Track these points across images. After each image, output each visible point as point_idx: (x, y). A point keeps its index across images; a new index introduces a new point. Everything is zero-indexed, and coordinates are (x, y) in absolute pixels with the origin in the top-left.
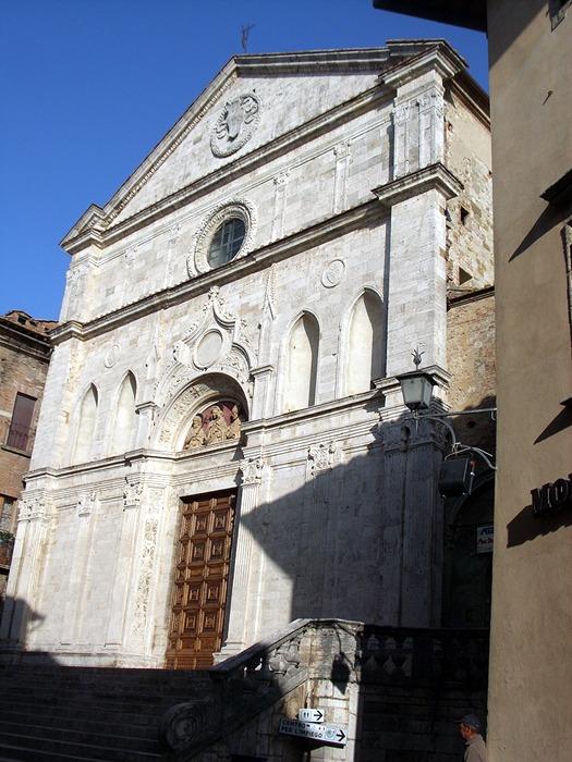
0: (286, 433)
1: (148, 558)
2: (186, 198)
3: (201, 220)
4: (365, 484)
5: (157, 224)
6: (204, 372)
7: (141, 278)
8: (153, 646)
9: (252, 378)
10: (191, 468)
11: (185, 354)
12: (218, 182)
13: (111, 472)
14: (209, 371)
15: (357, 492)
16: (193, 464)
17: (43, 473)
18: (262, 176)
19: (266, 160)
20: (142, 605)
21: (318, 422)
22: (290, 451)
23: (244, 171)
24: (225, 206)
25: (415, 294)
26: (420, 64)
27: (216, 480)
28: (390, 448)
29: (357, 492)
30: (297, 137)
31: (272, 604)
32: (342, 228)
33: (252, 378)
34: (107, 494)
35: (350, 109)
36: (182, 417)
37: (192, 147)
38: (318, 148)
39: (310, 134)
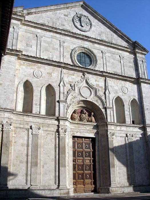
2: (68, 35)
4: (140, 146)
5: (55, 35)
6: (85, 99)
7: (46, 50)
10: (76, 127)
13: (48, 121)
14: (87, 99)
15: (138, 148)
16: (77, 126)
18: (96, 47)
19: (98, 44)
21: (127, 128)
23: (91, 41)
24: (85, 48)
26: (143, 53)
27: (87, 134)
29: (138, 148)
30: (110, 45)
31: (121, 173)
32: (127, 80)
37: (63, 16)
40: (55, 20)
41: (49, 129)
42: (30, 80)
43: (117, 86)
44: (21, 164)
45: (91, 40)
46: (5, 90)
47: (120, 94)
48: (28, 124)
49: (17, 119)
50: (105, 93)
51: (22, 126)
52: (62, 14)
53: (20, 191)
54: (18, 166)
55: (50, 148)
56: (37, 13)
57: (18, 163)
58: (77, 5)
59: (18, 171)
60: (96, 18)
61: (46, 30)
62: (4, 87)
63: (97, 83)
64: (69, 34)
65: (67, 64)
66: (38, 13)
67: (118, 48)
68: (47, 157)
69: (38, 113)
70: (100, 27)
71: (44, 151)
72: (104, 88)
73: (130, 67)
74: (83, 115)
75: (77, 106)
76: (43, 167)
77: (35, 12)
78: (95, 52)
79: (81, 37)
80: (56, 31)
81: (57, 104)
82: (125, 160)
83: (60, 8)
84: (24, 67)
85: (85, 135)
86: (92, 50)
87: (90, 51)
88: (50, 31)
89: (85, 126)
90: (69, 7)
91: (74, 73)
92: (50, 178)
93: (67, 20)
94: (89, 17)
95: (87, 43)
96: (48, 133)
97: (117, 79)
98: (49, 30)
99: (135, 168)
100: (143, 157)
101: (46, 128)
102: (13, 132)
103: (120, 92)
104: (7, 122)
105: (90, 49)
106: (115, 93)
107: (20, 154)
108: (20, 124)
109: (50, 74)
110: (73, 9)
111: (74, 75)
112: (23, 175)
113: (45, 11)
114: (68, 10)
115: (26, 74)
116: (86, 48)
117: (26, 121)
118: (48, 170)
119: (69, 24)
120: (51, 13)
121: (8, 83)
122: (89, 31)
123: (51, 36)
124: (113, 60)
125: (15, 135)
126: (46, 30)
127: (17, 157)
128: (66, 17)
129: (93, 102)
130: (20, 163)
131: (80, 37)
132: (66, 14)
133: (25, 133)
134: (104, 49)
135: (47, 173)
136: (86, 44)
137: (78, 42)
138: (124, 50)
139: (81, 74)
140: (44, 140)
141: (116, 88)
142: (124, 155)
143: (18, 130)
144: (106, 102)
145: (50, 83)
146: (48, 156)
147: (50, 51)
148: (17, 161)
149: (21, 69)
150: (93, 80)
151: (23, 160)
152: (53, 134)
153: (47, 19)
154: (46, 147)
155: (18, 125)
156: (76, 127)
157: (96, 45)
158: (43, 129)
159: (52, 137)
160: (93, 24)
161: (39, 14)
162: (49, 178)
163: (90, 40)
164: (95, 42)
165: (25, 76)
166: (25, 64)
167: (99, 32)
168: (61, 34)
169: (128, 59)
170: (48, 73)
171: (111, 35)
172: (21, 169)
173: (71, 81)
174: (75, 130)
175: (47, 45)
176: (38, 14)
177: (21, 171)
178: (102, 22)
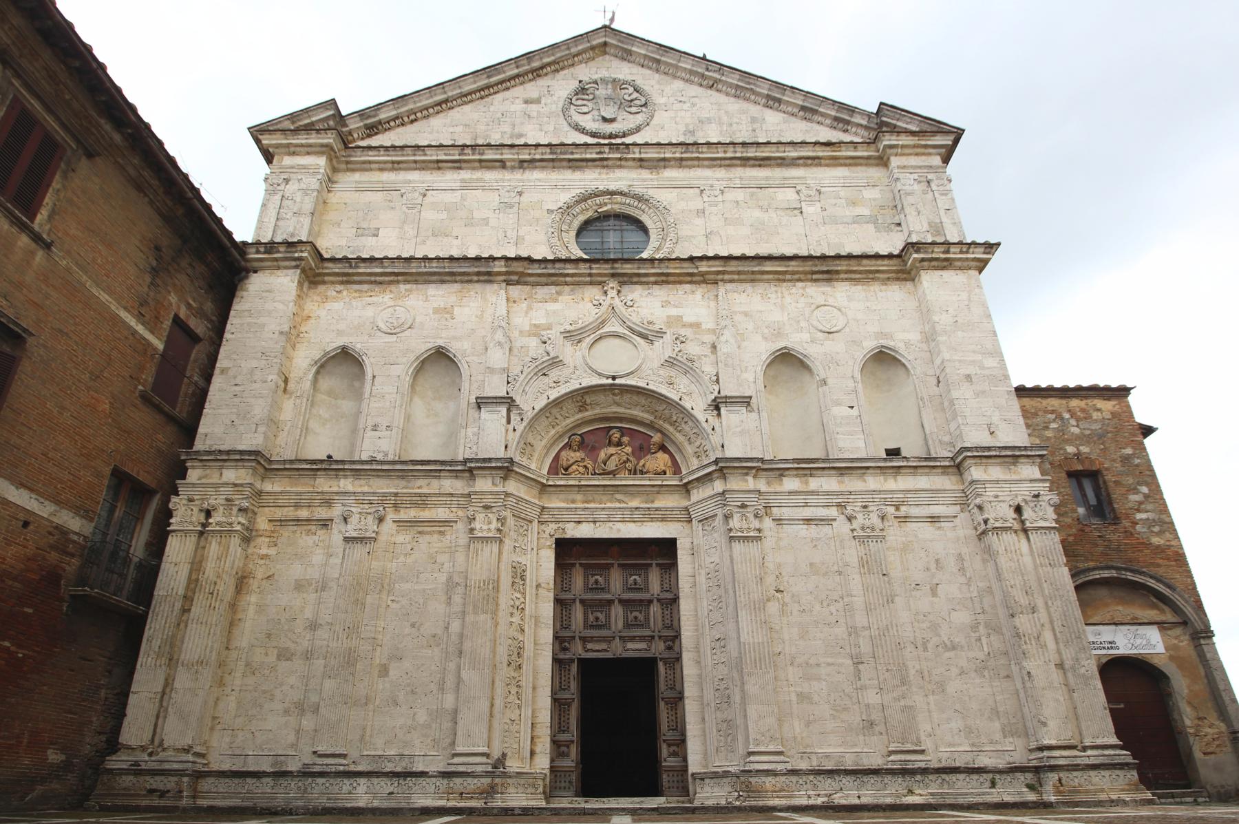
0: (791, 483)
1: (516, 619)
2: (532, 161)
3: (565, 197)
4: (937, 561)
6: (610, 381)
8: (532, 753)
9: (716, 406)
11: (571, 354)
12: (594, 160)
13: (420, 482)
16: (579, 497)
17: (225, 457)
18: (670, 179)
19: (681, 163)
20: (514, 691)
21: (846, 479)
22: (806, 505)
23: (641, 163)
24: (612, 193)
25: (982, 368)
27: (632, 525)
28: (997, 525)
31: (816, 698)
33: (716, 406)
34: (412, 514)
35: (820, 154)
36: (553, 432)
37: (518, 106)
38: (767, 179)
39: (755, 159)
40: (483, 128)
41: (426, 514)
42: (359, 346)
43: (783, 307)
44: (284, 665)
45: (643, 156)
46: (237, 388)
47: (797, 341)
48: (328, 503)
49: (288, 489)
50: (714, 347)
51: (304, 513)
52: (517, 101)
53: (248, 780)
54: (267, 672)
55: (424, 590)
56: (406, 119)
57: (272, 658)
58: (580, 48)
59: (264, 692)
60: (672, 72)
61: (441, 165)
62: (235, 377)
63: (673, 312)
64: (538, 157)
65: (518, 259)
66: (413, 117)
67: (783, 158)
68: (407, 630)
69: (380, 457)
70: (694, 105)
71: (394, 605)
72: (708, 324)
73: (858, 219)
74: (612, 450)
75: (580, 416)
76: (384, 671)
77: (397, 118)
78: (664, 197)
79: (594, 156)
80: (477, 157)
81: (473, 413)
82: (841, 631)
83: (502, 82)
84: (336, 306)
85: (619, 530)
86: (651, 192)
87: (640, 198)
88: (458, 165)
89: (618, 496)
90: (542, 68)
91: (559, 293)
92: (414, 720)
93: (534, 114)
94: (639, 82)
95: (619, 173)
96: (420, 529)
97: (780, 278)
98: (450, 165)
99: (912, 672)
100: (962, 617)
101: (412, 514)
102: (267, 540)
103: (801, 330)
104: (227, 500)
105: (639, 190)
106: (766, 339)
107: (283, 621)
108: (297, 506)
109: (447, 311)
110: (566, 72)
111: (556, 300)
112: (286, 712)
113: (439, 104)
114: (542, 82)
115: (342, 326)
116: (621, 194)
117: (322, 493)
118: (408, 685)
119: (545, 128)
120: (467, 108)
121: (254, 363)
122: (638, 129)
123: (463, 181)
124: (757, 213)
125: (272, 551)
126: (438, 165)
127: (269, 636)
128: (534, 107)
129: (650, 387)
130: (279, 657)
131: (588, 156)
132: (535, 95)
133: (316, 538)
134: (707, 179)
135: (401, 698)
136: (620, 179)
137: (580, 180)
138: (818, 158)
139: (593, 292)
140: (402, 559)
141: (777, 316)
142: (833, 609)
143: (286, 532)
144: (718, 381)
145: (441, 342)
146: (413, 625)
147: (455, 234)
148: (267, 654)
149: (323, 313)
150: (649, 304)
151: (292, 646)
152: (442, 533)
153: (452, 129)
154: (407, 586)
155: (289, 512)
156: (573, 502)
157: (672, 174)
158: (397, 517)
159: (439, 545)
160: (659, 100)
161: (415, 124)
162: (409, 722)
163: (637, 156)
164: (664, 159)
165: (340, 333)
166: (345, 293)
167: (687, 125)
168: (502, 164)
169: (842, 194)
170: (437, 311)
171: (754, 120)
172: (281, 684)
173: (543, 321)
174: (566, 515)
175: (444, 215)
176: (412, 122)
177: (277, 692)
178: (705, 83)
